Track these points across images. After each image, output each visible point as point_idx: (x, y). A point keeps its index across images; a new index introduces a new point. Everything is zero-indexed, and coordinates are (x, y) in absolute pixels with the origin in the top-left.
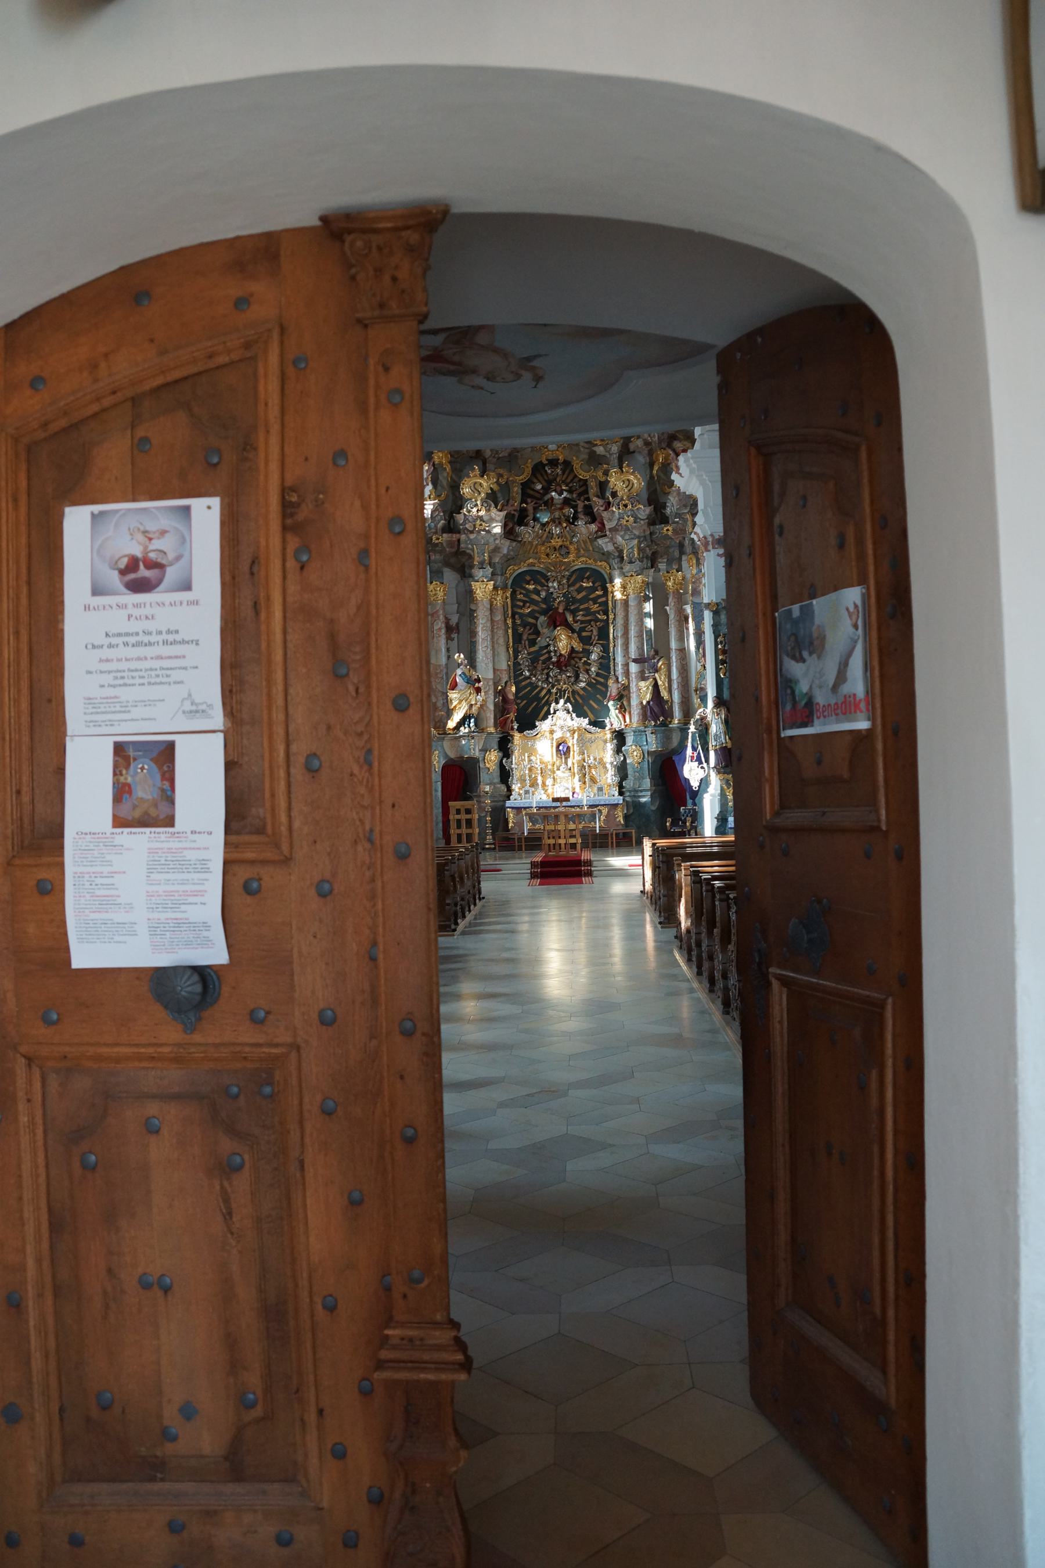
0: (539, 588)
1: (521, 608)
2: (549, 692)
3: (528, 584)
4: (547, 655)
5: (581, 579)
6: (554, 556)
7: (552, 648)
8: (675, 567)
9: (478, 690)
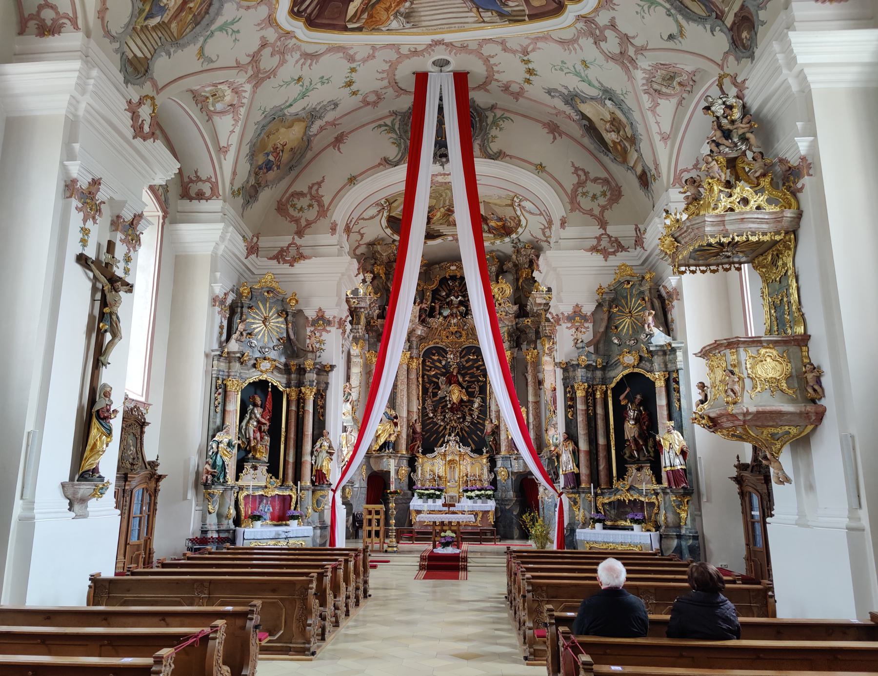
0: (441, 358)
1: (428, 371)
2: (445, 428)
3: (434, 355)
5: (468, 353)
7: (448, 399)
8: (533, 346)
9: (396, 424)
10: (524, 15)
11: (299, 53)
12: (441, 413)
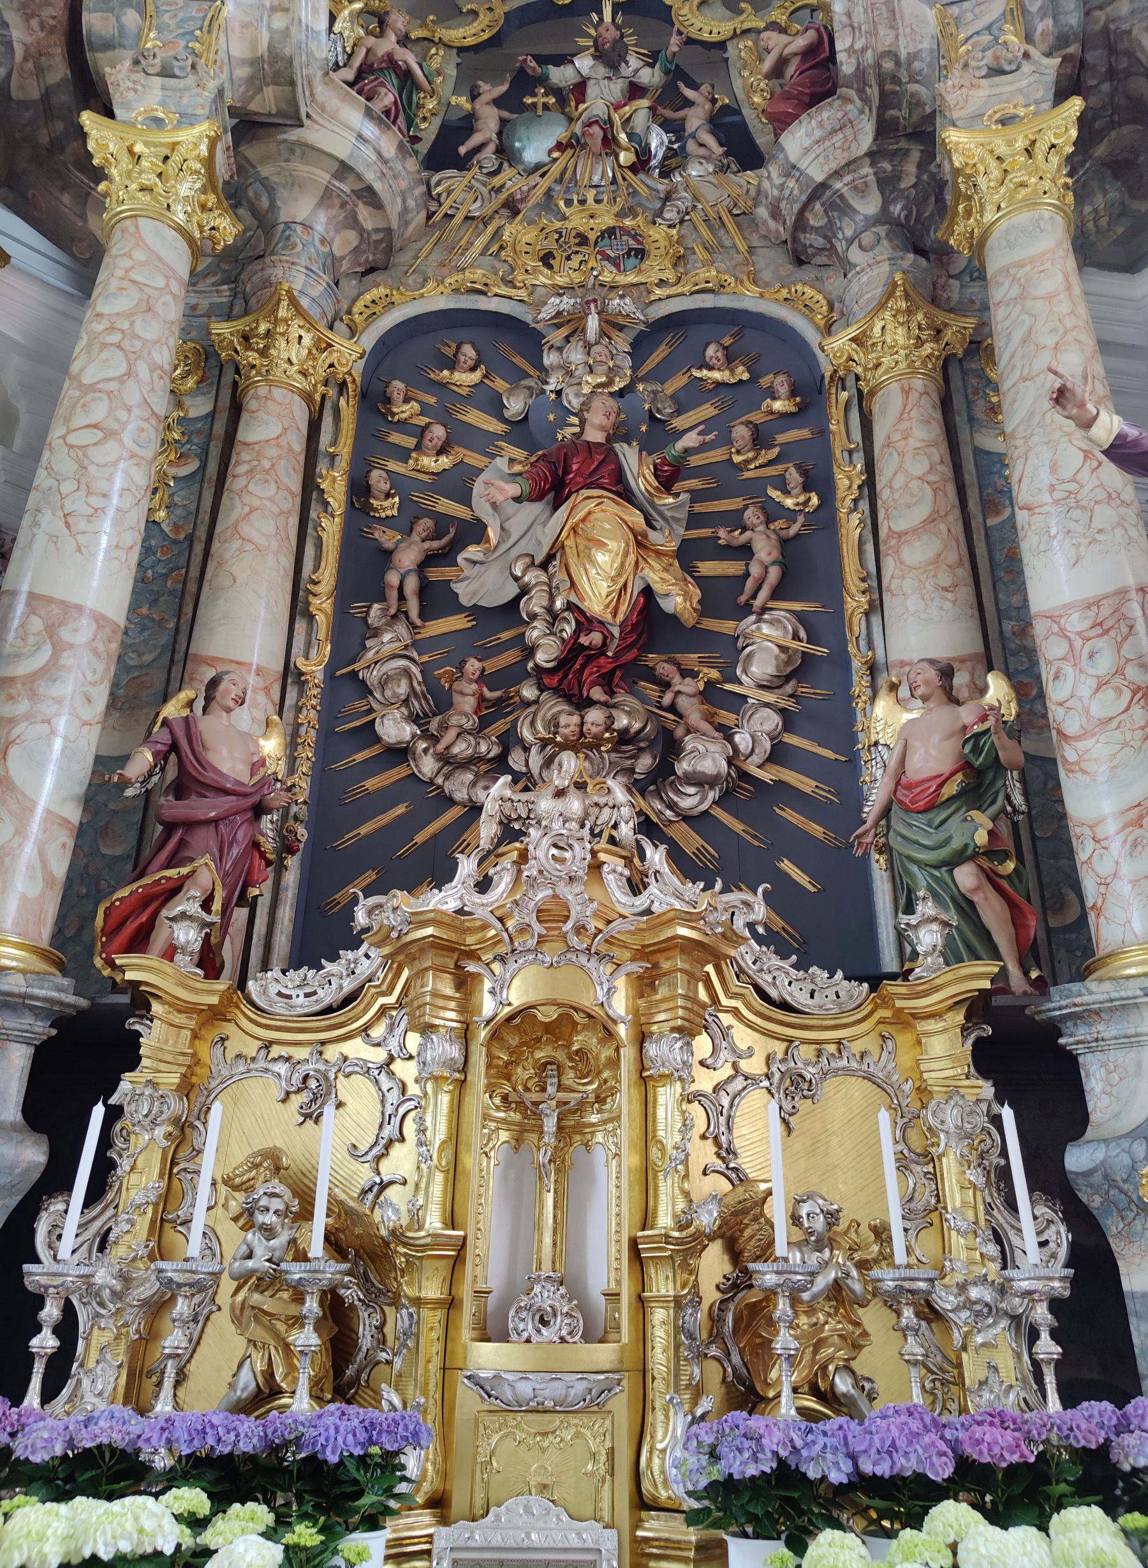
0: (500, 385)
1: (403, 455)
3: (452, 365)
4: (510, 657)
6: (574, 263)
12: (484, 723)
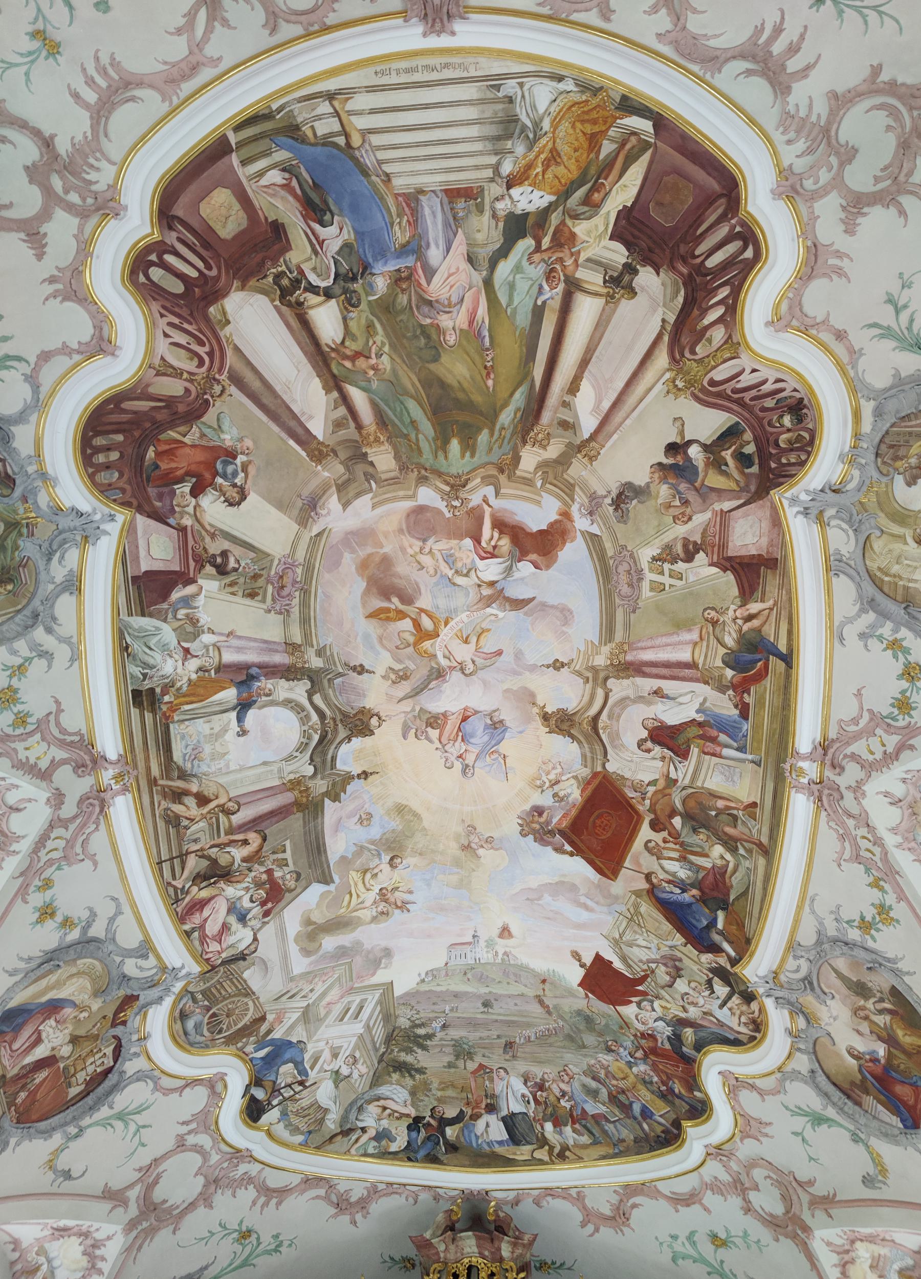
10: (241, 145)
11: (791, 99)
